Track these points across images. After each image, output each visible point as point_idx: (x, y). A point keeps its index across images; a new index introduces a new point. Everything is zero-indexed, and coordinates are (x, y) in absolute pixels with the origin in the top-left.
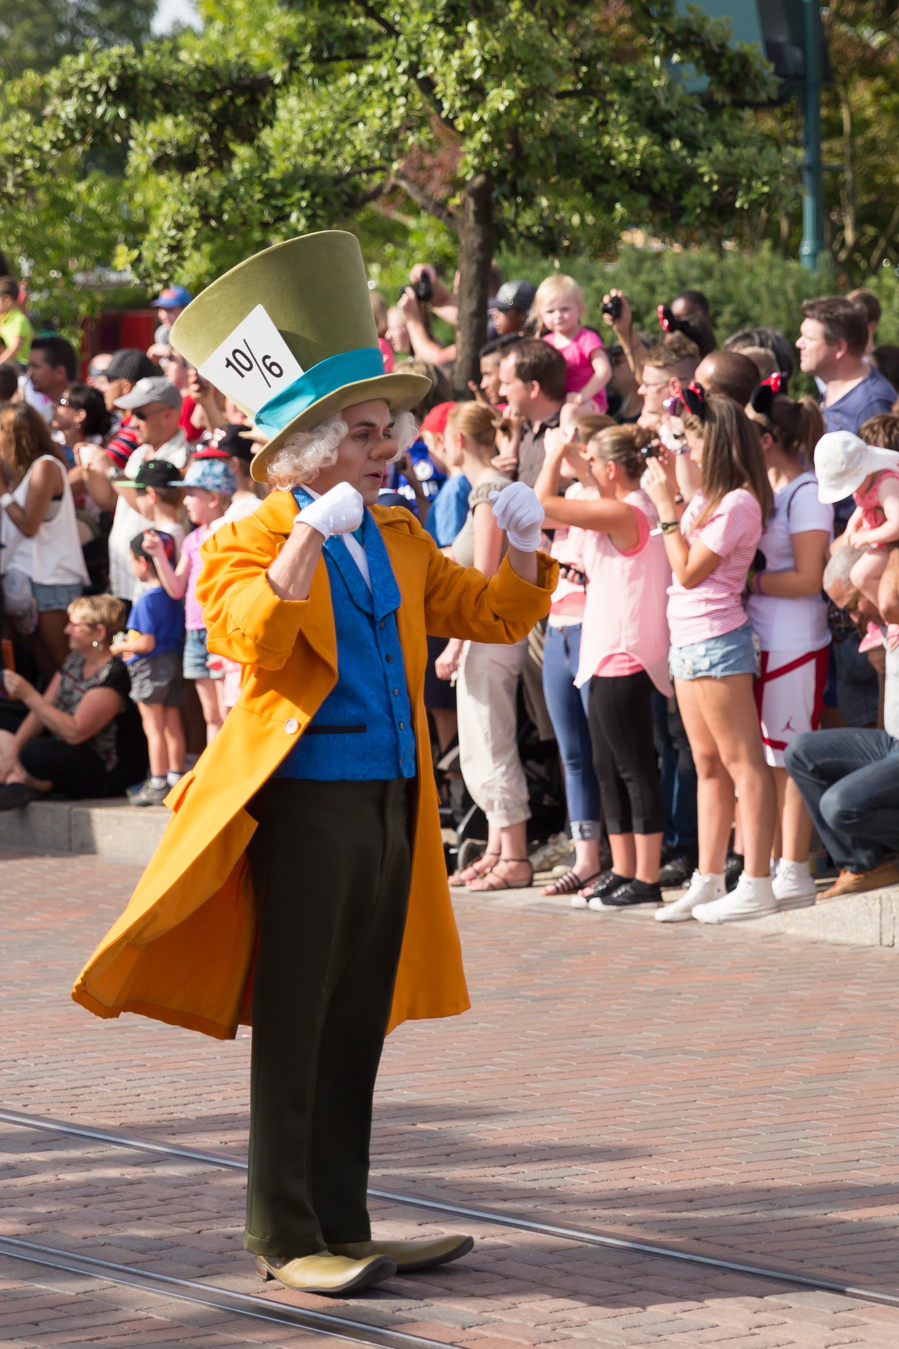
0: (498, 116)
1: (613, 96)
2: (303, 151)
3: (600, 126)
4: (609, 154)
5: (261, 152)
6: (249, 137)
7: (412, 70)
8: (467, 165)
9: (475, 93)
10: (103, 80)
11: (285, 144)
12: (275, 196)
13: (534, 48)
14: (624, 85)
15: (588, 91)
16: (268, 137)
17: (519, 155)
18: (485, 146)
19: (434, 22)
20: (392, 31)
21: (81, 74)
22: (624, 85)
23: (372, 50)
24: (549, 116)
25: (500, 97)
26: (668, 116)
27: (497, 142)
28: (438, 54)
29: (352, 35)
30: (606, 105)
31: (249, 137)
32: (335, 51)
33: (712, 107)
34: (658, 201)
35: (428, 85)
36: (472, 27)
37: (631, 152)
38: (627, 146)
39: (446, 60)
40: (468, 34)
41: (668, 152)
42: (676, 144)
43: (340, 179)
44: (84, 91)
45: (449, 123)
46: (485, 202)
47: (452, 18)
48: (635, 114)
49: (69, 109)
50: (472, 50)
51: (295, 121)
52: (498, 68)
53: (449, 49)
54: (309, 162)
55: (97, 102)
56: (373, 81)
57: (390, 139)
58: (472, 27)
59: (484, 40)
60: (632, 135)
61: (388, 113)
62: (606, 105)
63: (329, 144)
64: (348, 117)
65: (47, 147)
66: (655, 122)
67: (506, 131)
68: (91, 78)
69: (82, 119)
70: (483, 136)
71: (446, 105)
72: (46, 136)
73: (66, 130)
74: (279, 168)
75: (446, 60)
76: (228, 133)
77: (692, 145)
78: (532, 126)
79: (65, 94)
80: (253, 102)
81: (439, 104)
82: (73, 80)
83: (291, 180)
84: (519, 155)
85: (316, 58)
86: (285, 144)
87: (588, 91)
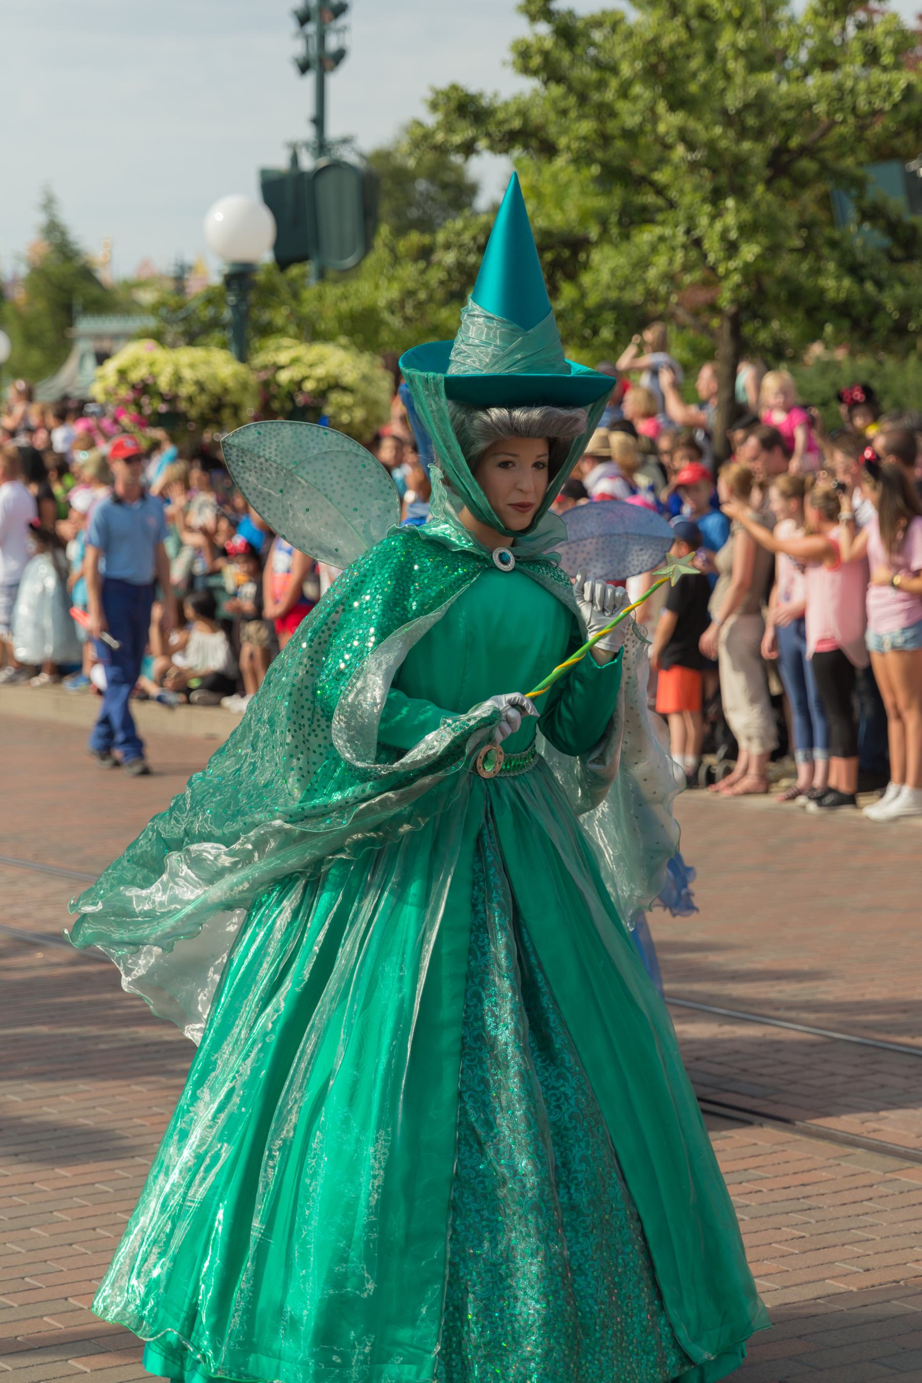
0: (747, 265)
1: (826, 251)
2: (609, 287)
3: (817, 271)
4: (822, 292)
5: (580, 287)
6: (572, 277)
7: (688, 232)
8: (725, 298)
9: (732, 248)
10: (474, 238)
11: (596, 283)
12: (592, 317)
13: (772, 217)
14: (833, 244)
15: (807, 249)
16: (586, 279)
17: (761, 291)
18: (738, 286)
19: (704, 200)
20: (672, 205)
21: (459, 234)
22: (833, 244)
23: (660, 217)
24: (784, 264)
25: (749, 252)
26: (863, 266)
27: (746, 282)
28: (704, 221)
29: (644, 209)
30: (819, 258)
31: (572, 277)
32: (634, 218)
33: (894, 260)
34: (856, 324)
35: (698, 243)
36: (730, 203)
37: (838, 289)
38: (834, 285)
39: (711, 224)
40: (726, 209)
41: (863, 291)
42: (869, 287)
43: (635, 307)
44: (461, 246)
45: (713, 269)
46: (736, 323)
47: (716, 197)
48: (840, 264)
49: (450, 258)
50: (730, 219)
51: (605, 267)
52: (748, 230)
53: (714, 218)
54: (613, 295)
55: (469, 253)
56: (662, 239)
57: (670, 278)
58: (730, 203)
59: (738, 211)
60: (839, 278)
61: (671, 261)
62: (819, 258)
63: (627, 284)
64: (643, 264)
65: (434, 283)
66: (854, 270)
67: (753, 276)
68: (466, 238)
69: (460, 265)
70: (736, 278)
71: (711, 258)
72: (435, 276)
73: (449, 273)
74: (592, 300)
75: (711, 224)
76: (559, 275)
77: (880, 285)
78: (769, 272)
79: (448, 247)
80: (575, 254)
81: (705, 256)
82: (453, 238)
83: (603, 306)
84: (761, 291)
85: (620, 223)
86: (596, 283)
87: (807, 249)
